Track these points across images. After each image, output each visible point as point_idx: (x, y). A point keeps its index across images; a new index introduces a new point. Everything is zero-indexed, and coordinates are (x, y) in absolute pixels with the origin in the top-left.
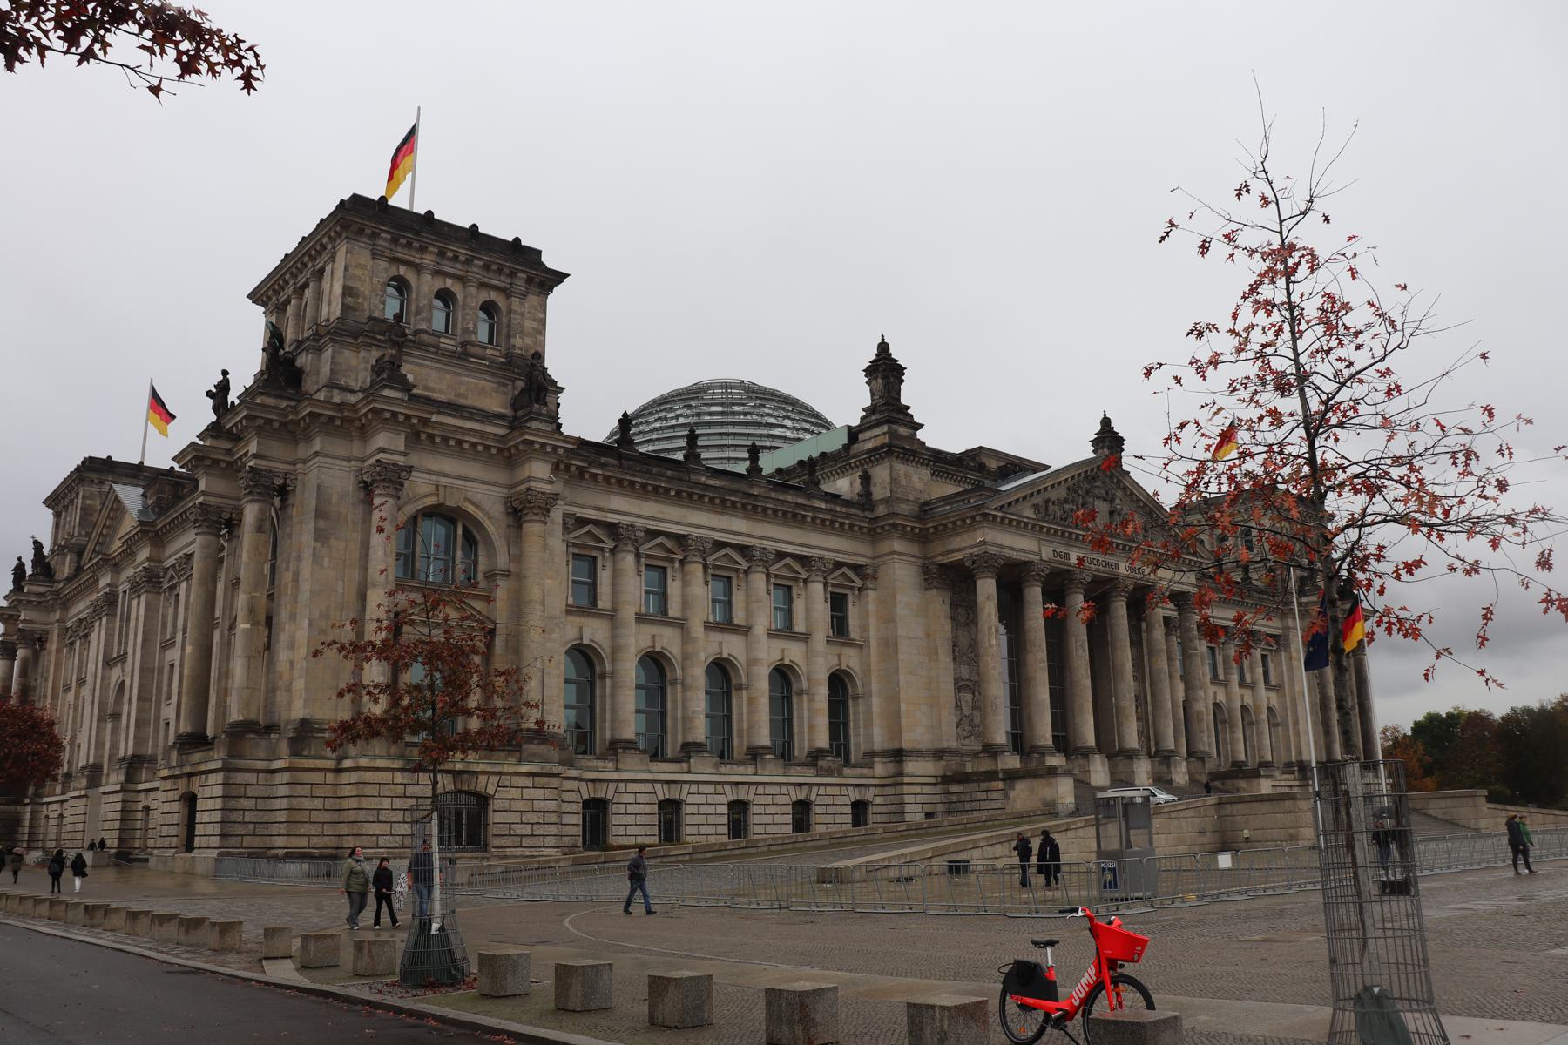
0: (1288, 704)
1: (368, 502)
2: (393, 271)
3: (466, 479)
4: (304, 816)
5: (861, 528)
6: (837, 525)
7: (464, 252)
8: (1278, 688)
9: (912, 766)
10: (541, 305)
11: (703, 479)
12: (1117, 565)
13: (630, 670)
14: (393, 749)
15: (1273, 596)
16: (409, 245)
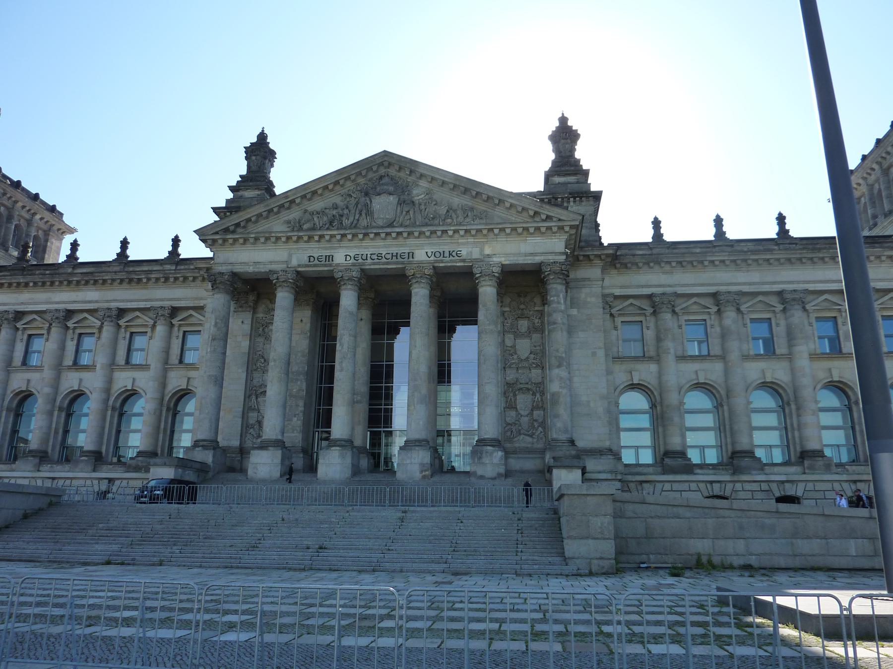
6: (172, 280)
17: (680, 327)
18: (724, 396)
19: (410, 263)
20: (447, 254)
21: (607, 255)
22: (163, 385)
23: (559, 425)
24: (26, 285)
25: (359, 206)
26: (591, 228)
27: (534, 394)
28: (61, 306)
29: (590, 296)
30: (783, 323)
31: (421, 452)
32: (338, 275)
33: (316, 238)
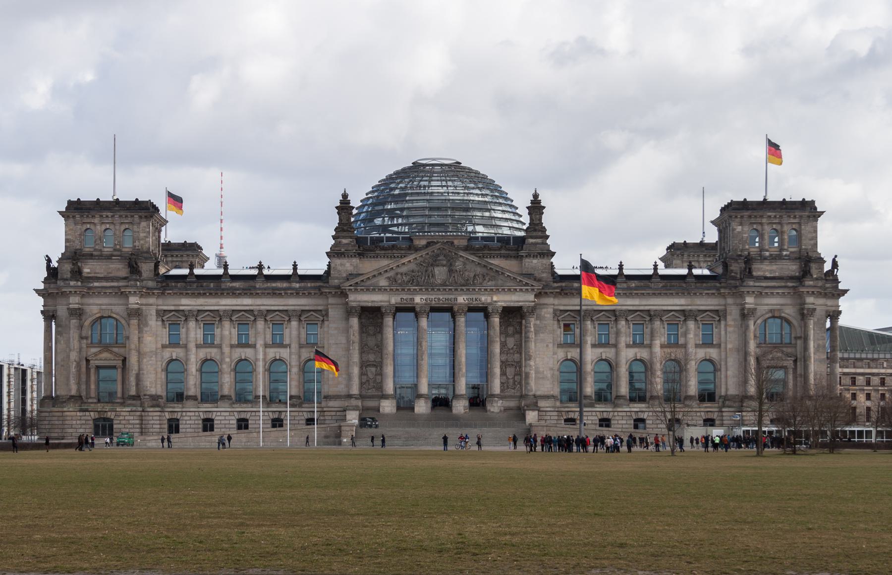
0: (723, 357)
1: (70, 322)
2: (85, 227)
3: (111, 305)
4: (54, 427)
5: (315, 293)
6: (301, 294)
7: (110, 214)
8: (719, 346)
9: (332, 403)
10: (147, 225)
11: (228, 284)
12: (456, 299)
13: (193, 368)
14: (77, 405)
15: (720, 283)
16: (87, 216)
17: (595, 328)
18: (615, 367)
19: (456, 304)
20: (474, 300)
21: (557, 292)
22: (300, 357)
23: (529, 388)
24: (205, 294)
25: (428, 272)
26: (549, 273)
27: (516, 367)
28: (227, 308)
29: (547, 313)
30: (649, 326)
31: (464, 401)
32: (418, 309)
33: (406, 290)
